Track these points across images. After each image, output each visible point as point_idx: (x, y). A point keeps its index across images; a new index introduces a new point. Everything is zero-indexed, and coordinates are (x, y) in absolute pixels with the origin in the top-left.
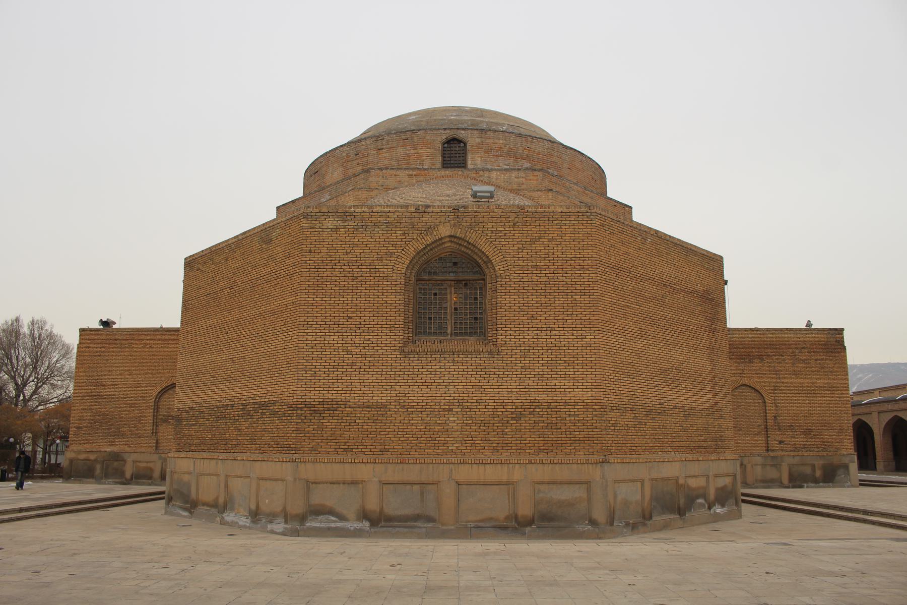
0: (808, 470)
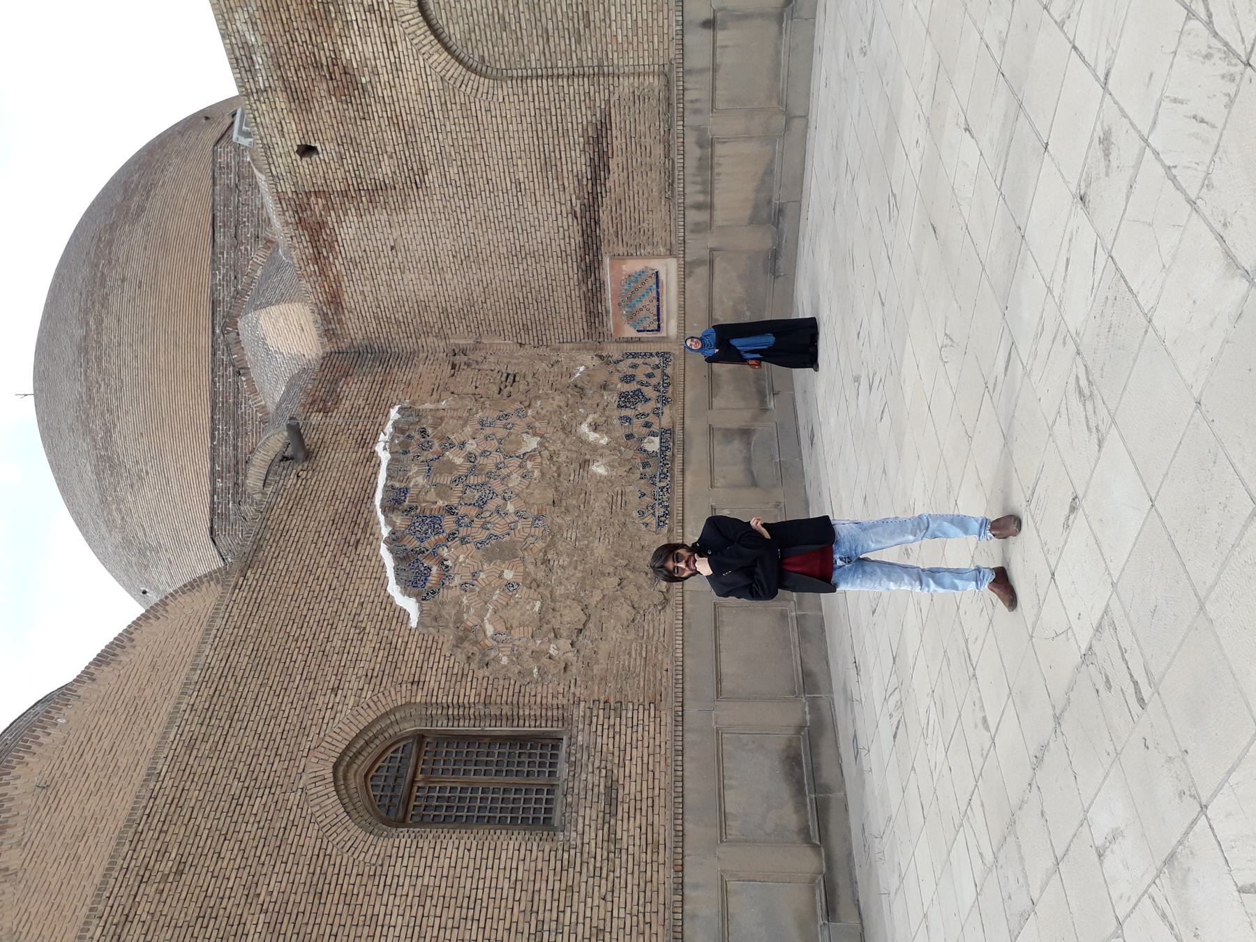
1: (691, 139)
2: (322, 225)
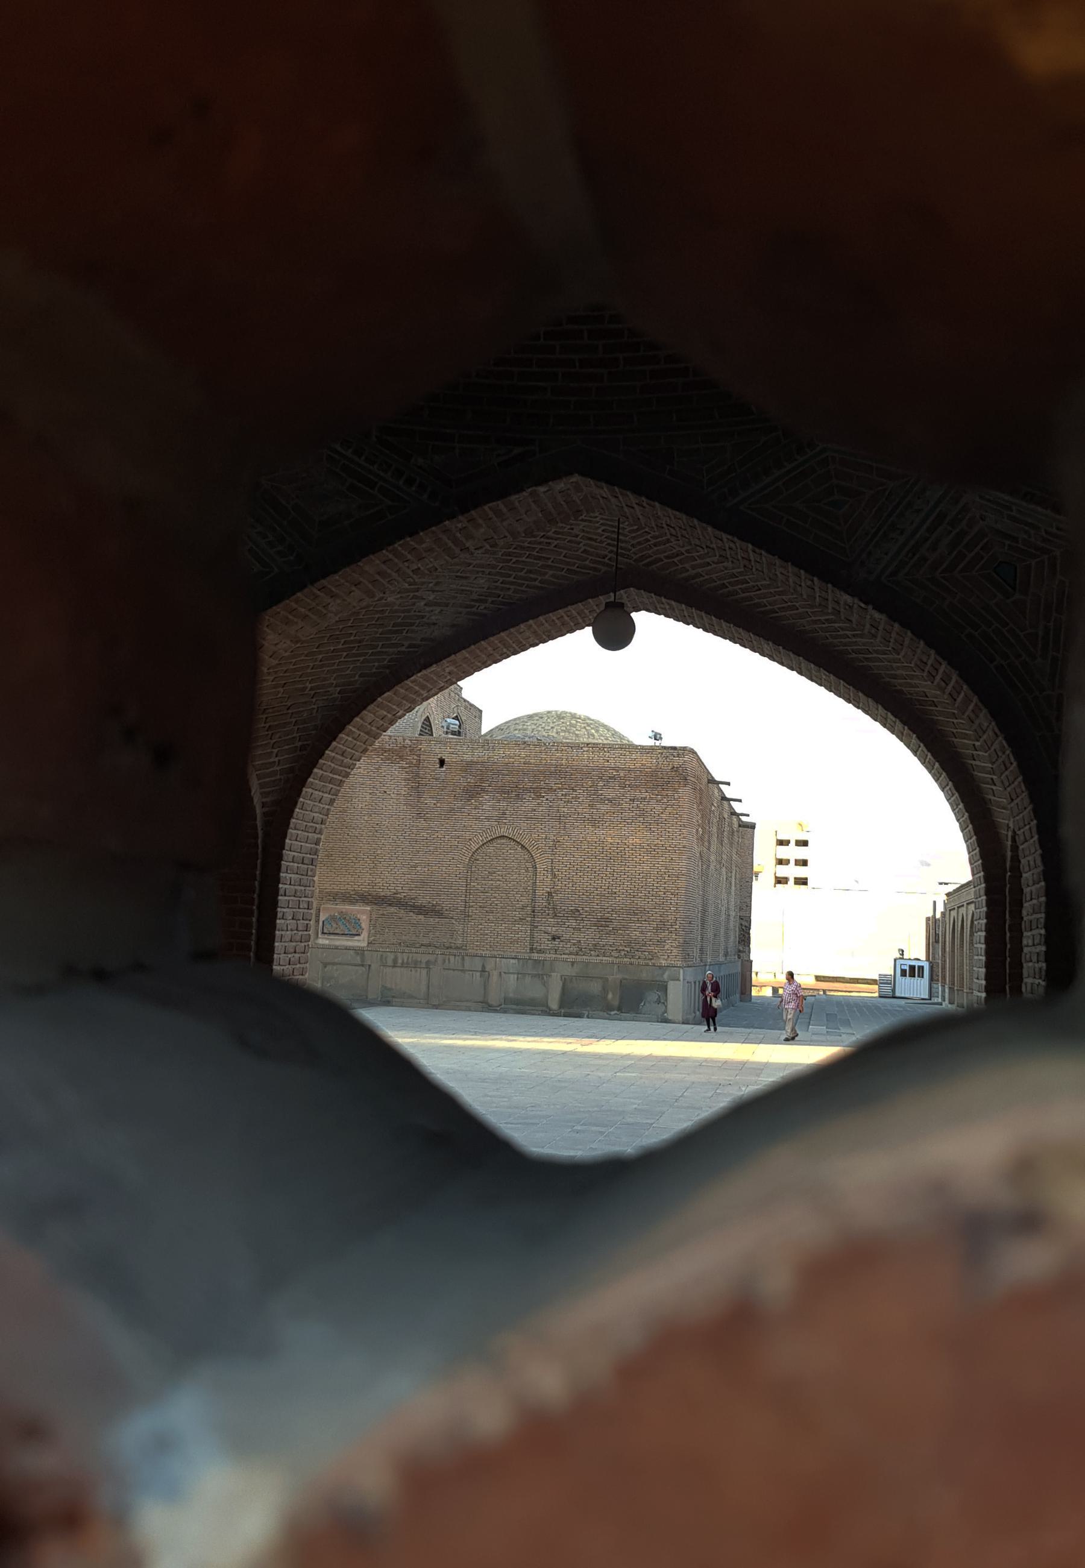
0: (595, 988)
1: (432, 958)
2: (401, 758)
